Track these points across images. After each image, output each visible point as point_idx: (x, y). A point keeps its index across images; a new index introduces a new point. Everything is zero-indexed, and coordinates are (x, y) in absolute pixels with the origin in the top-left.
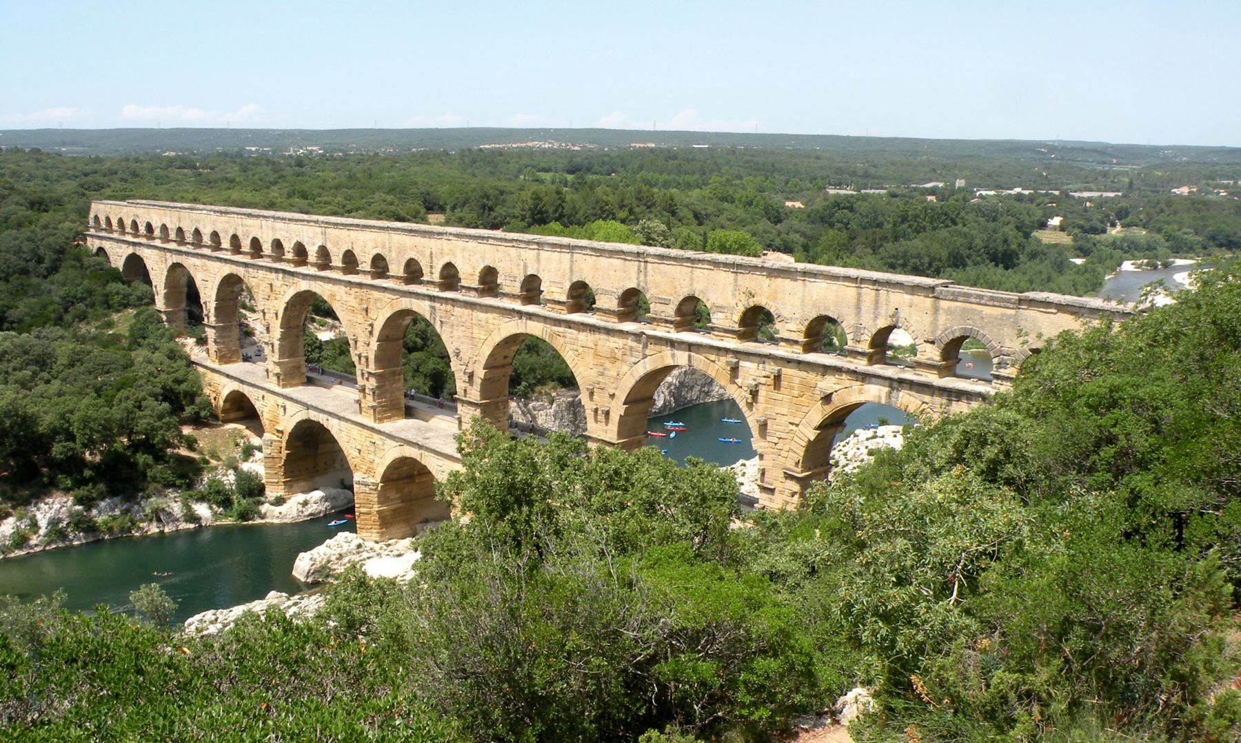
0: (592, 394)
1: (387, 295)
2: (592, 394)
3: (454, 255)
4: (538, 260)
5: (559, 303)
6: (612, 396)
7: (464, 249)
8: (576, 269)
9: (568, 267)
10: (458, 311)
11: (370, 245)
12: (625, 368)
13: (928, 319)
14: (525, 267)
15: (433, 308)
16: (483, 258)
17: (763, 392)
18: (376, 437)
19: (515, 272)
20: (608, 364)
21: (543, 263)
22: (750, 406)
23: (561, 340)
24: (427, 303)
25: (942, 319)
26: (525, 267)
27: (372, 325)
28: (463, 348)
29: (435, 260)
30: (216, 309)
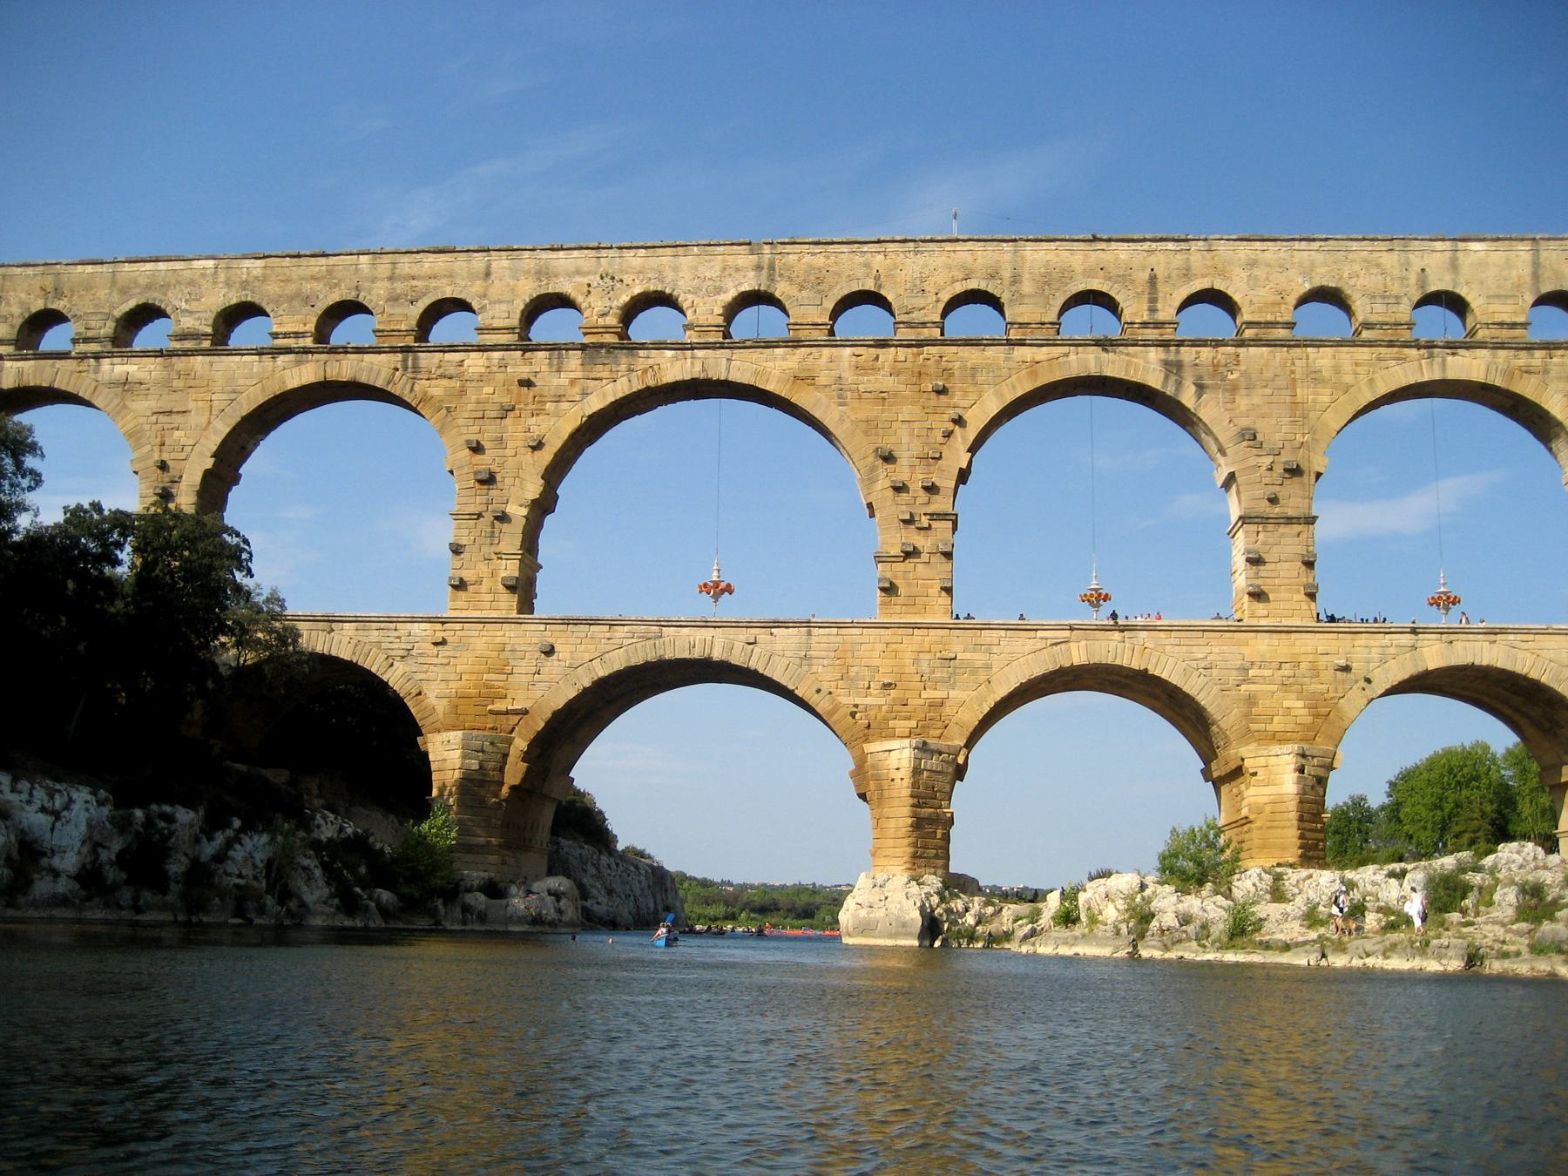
3: (1223, 274)
4: (1454, 266)
5: (1513, 326)
8: (1546, 274)
9: (1526, 272)
11: (941, 278)
14: (1422, 282)
15: (1173, 368)
16: (1307, 273)
18: (958, 644)
19: (1395, 289)
23: (1534, 379)
24: (1155, 354)
26: (1422, 282)
28: (1263, 428)
30: (208, 475)
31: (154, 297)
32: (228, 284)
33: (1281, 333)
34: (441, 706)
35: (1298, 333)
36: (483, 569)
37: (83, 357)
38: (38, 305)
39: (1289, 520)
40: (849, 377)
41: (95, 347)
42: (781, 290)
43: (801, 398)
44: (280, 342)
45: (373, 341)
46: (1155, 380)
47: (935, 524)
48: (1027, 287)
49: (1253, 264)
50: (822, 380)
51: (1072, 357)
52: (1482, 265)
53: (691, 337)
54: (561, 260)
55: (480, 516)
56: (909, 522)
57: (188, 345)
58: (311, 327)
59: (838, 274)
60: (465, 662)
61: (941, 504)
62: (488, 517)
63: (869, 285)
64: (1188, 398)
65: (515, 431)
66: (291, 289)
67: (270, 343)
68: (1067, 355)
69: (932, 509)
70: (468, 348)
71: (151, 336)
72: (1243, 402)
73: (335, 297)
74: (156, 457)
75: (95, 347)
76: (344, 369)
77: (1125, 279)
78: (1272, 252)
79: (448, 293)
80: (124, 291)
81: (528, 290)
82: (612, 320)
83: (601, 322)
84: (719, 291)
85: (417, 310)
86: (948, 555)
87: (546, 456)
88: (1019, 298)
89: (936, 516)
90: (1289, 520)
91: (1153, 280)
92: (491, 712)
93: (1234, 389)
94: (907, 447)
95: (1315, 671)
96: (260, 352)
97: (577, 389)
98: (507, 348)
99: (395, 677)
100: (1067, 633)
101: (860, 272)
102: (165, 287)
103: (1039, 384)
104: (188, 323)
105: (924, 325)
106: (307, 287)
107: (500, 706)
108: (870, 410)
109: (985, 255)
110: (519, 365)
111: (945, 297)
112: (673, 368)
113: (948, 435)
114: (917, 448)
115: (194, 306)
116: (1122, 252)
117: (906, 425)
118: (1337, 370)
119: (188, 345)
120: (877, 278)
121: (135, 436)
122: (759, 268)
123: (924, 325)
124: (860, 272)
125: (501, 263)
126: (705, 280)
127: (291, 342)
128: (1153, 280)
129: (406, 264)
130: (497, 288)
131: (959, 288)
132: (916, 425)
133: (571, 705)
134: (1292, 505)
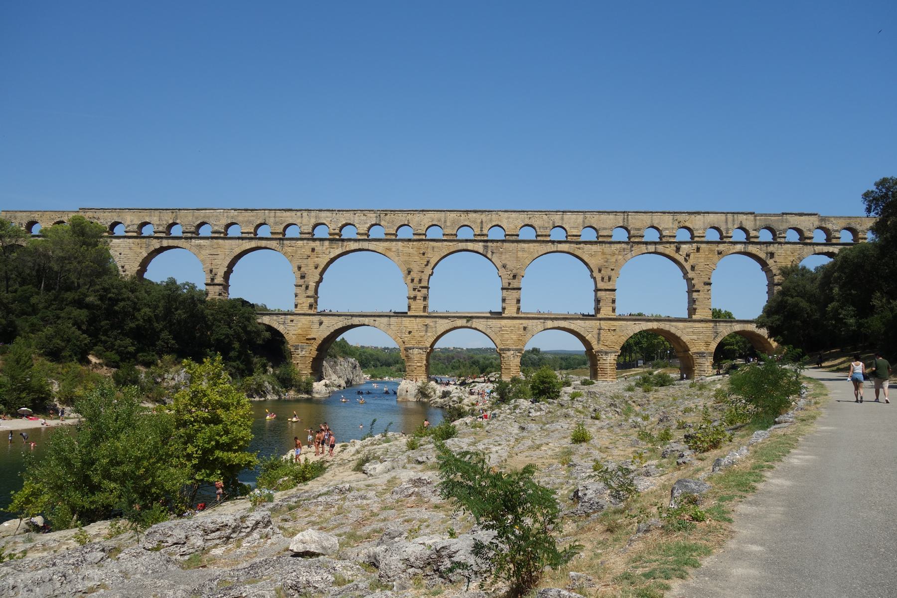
0: (600, 271)
1: (445, 243)
2: (600, 271)
4: (562, 219)
6: (612, 270)
7: (509, 218)
10: (506, 245)
12: (620, 257)
13: (753, 223)
14: (554, 223)
15: (486, 247)
17: (692, 256)
20: (609, 257)
21: (565, 220)
22: (686, 260)
24: (481, 244)
25: (758, 223)
26: (554, 223)
27: (428, 262)
28: (508, 263)
29: (484, 224)
31: (206, 220)
32: (227, 217)
33: (514, 238)
34: (294, 337)
35: (520, 238)
36: (305, 300)
37: (186, 238)
38: (171, 222)
39: (514, 289)
40: (401, 249)
41: (189, 235)
42: (382, 223)
43: (389, 254)
44: (244, 235)
45: (270, 236)
46: (481, 251)
48: (448, 224)
49: (509, 218)
52: (570, 218)
53: (359, 237)
54: (323, 214)
55: (301, 286)
56: (414, 289)
57: (216, 235)
58: (252, 231)
60: (300, 325)
61: (424, 284)
62: (304, 287)
64: (489, 255)
65: (311, 263)
66: (246, 219)
67: (240, 235)
70: (297, 239)
71: (205, 231)
72: (503, 257)
73: (258, 222)
74: (210, 267)
75: (189, 235)
76: (263, 243)
77: (474, 222)
78: (514, 215)
79: (291, 221)
80: (197, 218)
81: (313, 221)
82: (337, 231)
83: (333, 232)
84: (366, 223)
85: (282, 227)
86: (425, 298)
87: (320, 269)
88: (446, 227)
89: (422, 287)
90: (514, 289)
91: (482, 222)
92: (308, 339)
93: (502, 253)
94: (416, 268)
95: (519, 328)
96: (239, 238)
97: (327, 252)
98: (308, 239)
99: (281, 328)
101: (404, 219)
102: (209, 217)
104: (216, 228)
105: (420, 234)
106: (251, 218)
107: (309, 337)
108: (406, 258)
109: (437, 215)
110: (312, 244)
112: (353, 246)
114: (418, 268)
115: (218, 223)
116: (474, 215)
118: (529, 248)
119: (216, 235)
121: (203, 261)
123: (420, 234)
124: (404, 219)
125: (305, 214)
126: (362, 223)
127: (246, 235)
128: (482, 222)
129: (279, 213)
130: (305, 219)
133: (328, 336)
134: (515, 284)
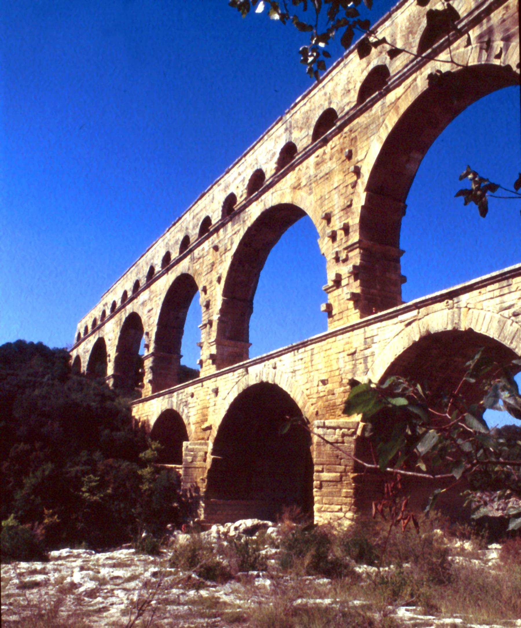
27: (357, 172)
30: (157, 334)
47: (351, 254)
50: (303, 184)
51: (418, 80)
59: (314, 109)
63: (326, 106)
68: (415, 80)
69: (350, 243)
84: (274, 154)
89: (350, 248)
100: (415, 312)
103: (399, 116)
111: (359, 85)
113: (354, 185)
117: (337, 190)
120: (330, 99)
122: (286, 129)
131: (366, 74)
132: (341, 187)
